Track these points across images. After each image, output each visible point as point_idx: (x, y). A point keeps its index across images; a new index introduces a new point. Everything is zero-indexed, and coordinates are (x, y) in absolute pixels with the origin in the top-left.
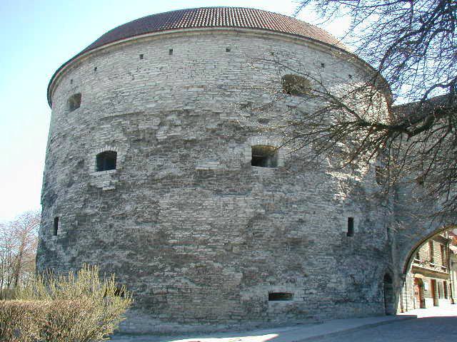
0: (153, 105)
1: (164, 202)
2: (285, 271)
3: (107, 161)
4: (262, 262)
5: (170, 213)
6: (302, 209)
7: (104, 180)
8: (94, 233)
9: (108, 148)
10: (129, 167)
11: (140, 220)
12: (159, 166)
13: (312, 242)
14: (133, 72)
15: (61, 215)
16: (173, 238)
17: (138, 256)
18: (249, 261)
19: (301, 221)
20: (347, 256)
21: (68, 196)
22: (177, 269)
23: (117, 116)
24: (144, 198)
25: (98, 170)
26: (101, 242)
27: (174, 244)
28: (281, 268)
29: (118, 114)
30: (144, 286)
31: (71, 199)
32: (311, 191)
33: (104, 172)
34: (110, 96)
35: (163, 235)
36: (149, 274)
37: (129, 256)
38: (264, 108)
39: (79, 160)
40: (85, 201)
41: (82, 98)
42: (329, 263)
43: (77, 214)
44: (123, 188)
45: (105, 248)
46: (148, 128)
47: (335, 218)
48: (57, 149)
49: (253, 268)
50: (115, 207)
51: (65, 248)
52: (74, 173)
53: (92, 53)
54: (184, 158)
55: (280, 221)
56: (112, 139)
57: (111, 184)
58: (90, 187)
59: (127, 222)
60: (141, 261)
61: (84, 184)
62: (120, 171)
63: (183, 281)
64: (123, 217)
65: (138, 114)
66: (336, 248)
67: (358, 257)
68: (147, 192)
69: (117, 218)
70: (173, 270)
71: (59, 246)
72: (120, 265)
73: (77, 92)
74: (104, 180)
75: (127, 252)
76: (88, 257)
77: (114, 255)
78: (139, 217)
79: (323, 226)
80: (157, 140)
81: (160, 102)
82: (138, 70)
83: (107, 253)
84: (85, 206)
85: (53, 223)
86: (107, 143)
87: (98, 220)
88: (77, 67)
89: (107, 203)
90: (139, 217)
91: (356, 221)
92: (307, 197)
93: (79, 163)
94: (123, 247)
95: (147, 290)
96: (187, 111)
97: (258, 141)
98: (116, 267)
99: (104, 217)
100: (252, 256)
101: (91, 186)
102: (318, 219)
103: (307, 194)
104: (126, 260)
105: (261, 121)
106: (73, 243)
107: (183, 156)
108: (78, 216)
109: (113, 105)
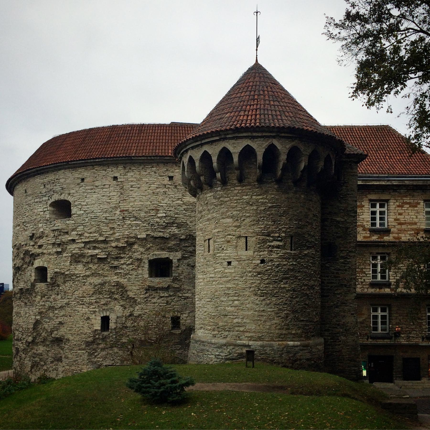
2: (52, 362)
4: (41, 355)
6: (62, 314)
13: (68, 340)
18: (35, 354)
19: (61, 323)
20: (103, 349)
28: (50, 359)
32: (68, 299)
38: (41, 237)
42: (81, 356)
47: (88, 318)
49: (36, 359)
55: (48, 325)
66: (88, 344)
67: (116, 350)
79: (77, 326)
91: (113, 317)
92: (66, 304)
97: (38, 263)
100: (37, 350)
102: (72, 320)
103: (66, 301)
105: (40, 247)
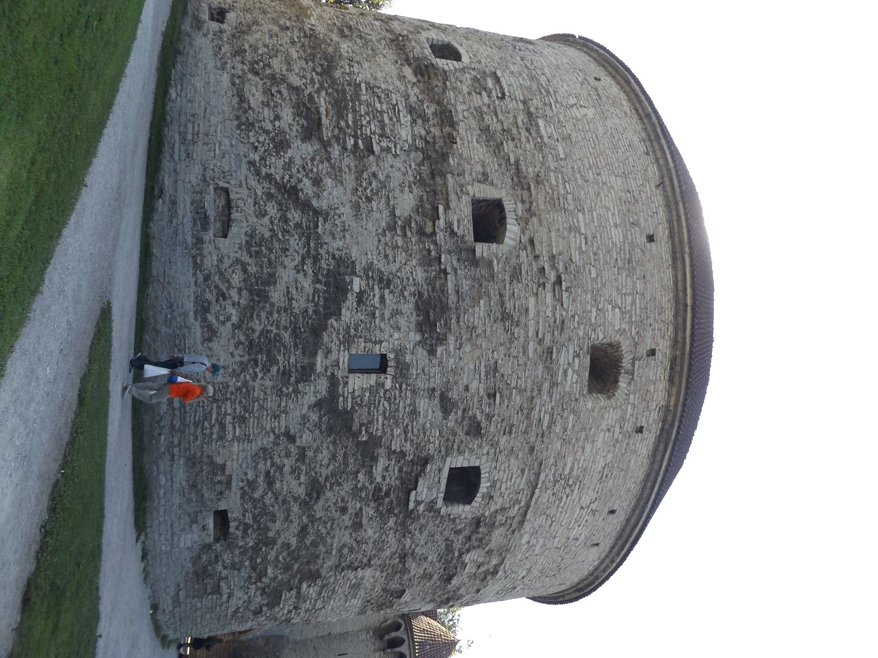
0: (524, 541)
1: (368, 572)
3: (464, 484)
5: (348, 579)
7: (430, 489)
8: (335, 479)
9: (484, 487)
10: (438, 522)
11: (346, 551)
12: (426, 559)
14: (593, 506)
15: (388, 384)
16: (309, 586)
17: (285, 554)
21: (423, 404)
22: (258, 593)
23: (533, 493)
24: (381, 550)
25: (451, 469)
26: (318, 498)
27: (299, 588)
29: (536, 496)
30: (234, 567)
31: (414, 413)
33: (443, 487)
34: (575, 473)
35: (313, 577)
36: (254, 568)
37: (287, 545)
39: (483, 425)
40: (403, 454)
41: (602, 400)
43: (381, 437)
44: (405, 517)
45: (306, 505)
46: (490, 540)
48: (531, 333)
50: (377, 510)
51: (318, 404)
52: (464, 410)
53: (672, 425)
54: (427, 576)
56: (496, 495)
57: (418, 503)
58: (426, 461)
59: (347, 533)
60: (277, 558)
61: (431, 449)
62: (438, 511)
63: (241, 602)
64: (357, 526)
65: (522, 523)
68: (388, 553)
69: (356, 515)
70: (257, 589)
71: (323, 386)
72: (271, 534)
73: (622, 384)
74: (430, 489)
75: (294, 542)
76: (293, 471)
77: (291, 521)
78: (351, 550)
80: (468, 551)
81: (526, 546)
82: (594, 512)
83: (295, 508)
84: (390, 453)
85: (377, 350)
86: (493, 486)
87: (359, 485)
88: (672, 368)
89: (387, 494)
90: (351, 550)
93: (479, 424)
94: (303, 531)
95: (225, 573)
96: (495, 572)
98: (268, 529)
99: (363, 495)
101: (426, 463)
104: (280, 542)
106: (324, 427)
107: (431, 576)
108: (375, 442)
109: (556, 482)
